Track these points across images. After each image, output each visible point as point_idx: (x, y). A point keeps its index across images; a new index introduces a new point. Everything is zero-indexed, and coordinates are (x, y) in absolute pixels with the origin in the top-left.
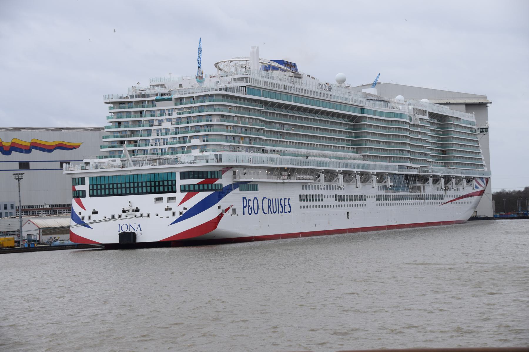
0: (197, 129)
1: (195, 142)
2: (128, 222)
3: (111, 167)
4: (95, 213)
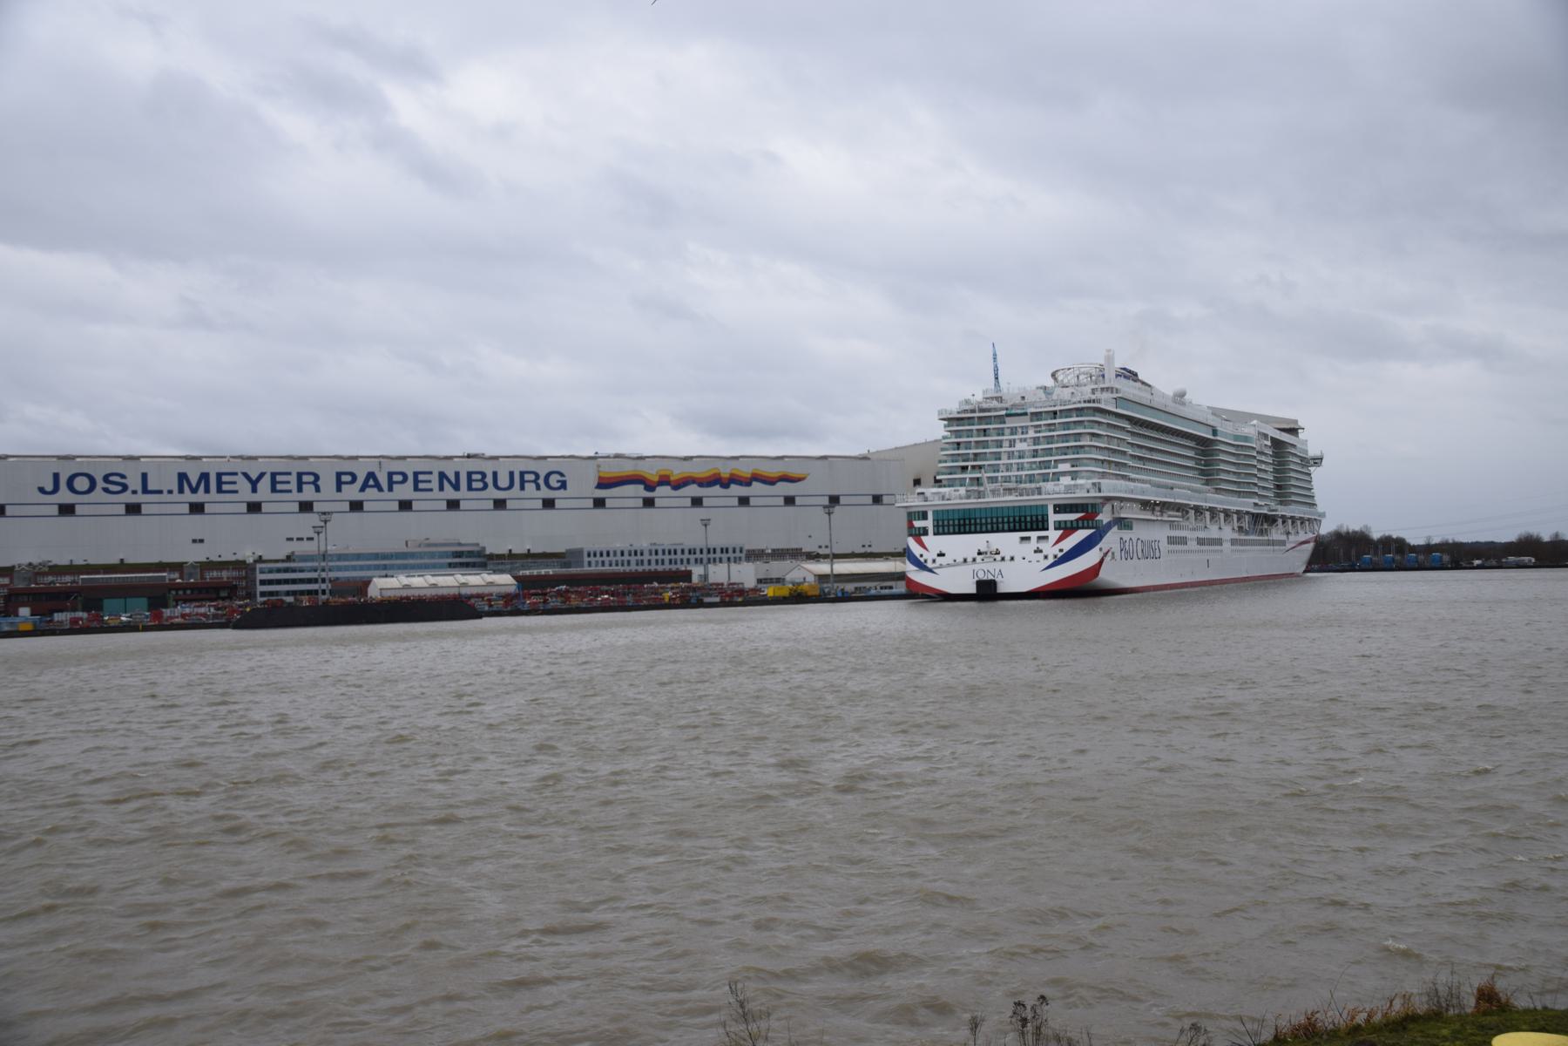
0: (1064, 451)
1: (1063, 467)
2: (985, 566)
3: (956, 497)
4: (941, 555)
